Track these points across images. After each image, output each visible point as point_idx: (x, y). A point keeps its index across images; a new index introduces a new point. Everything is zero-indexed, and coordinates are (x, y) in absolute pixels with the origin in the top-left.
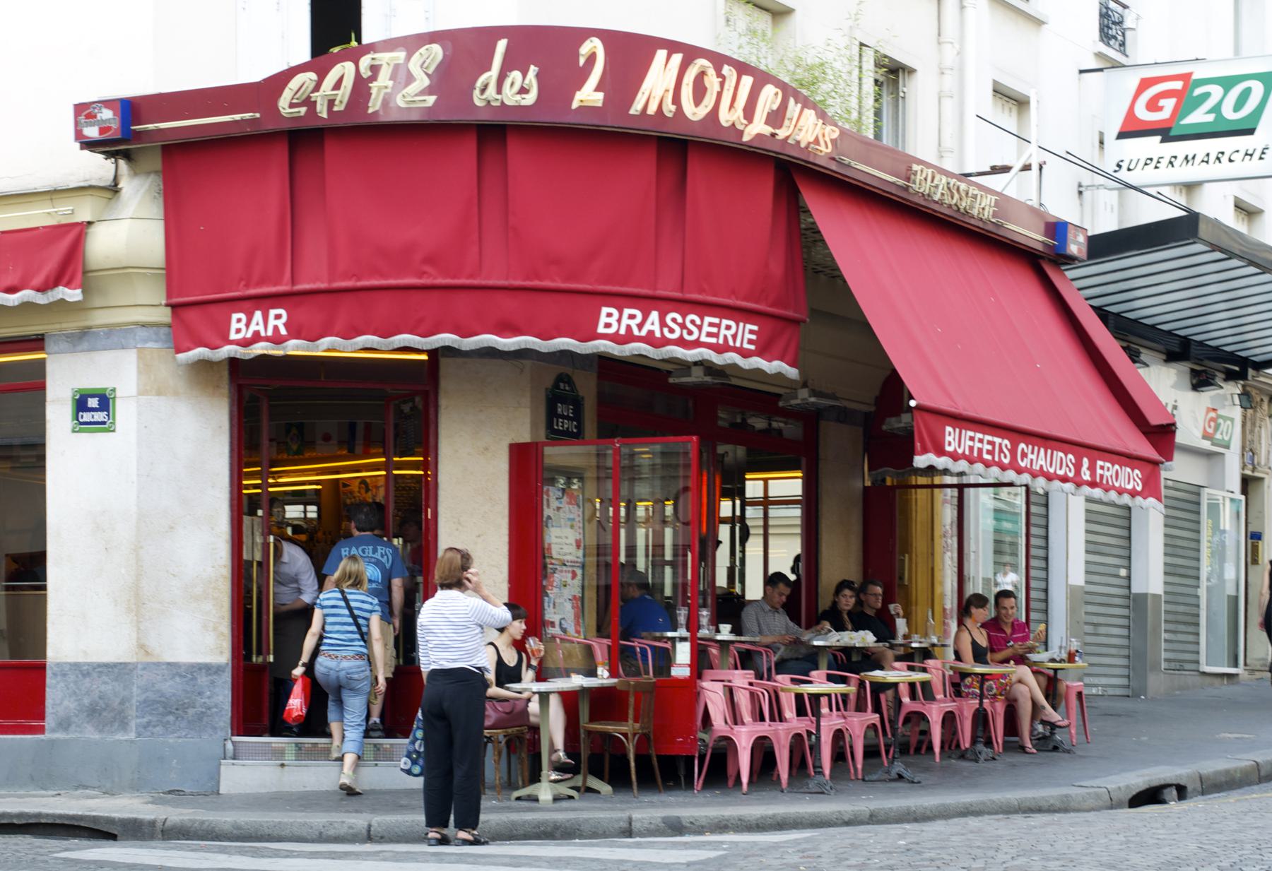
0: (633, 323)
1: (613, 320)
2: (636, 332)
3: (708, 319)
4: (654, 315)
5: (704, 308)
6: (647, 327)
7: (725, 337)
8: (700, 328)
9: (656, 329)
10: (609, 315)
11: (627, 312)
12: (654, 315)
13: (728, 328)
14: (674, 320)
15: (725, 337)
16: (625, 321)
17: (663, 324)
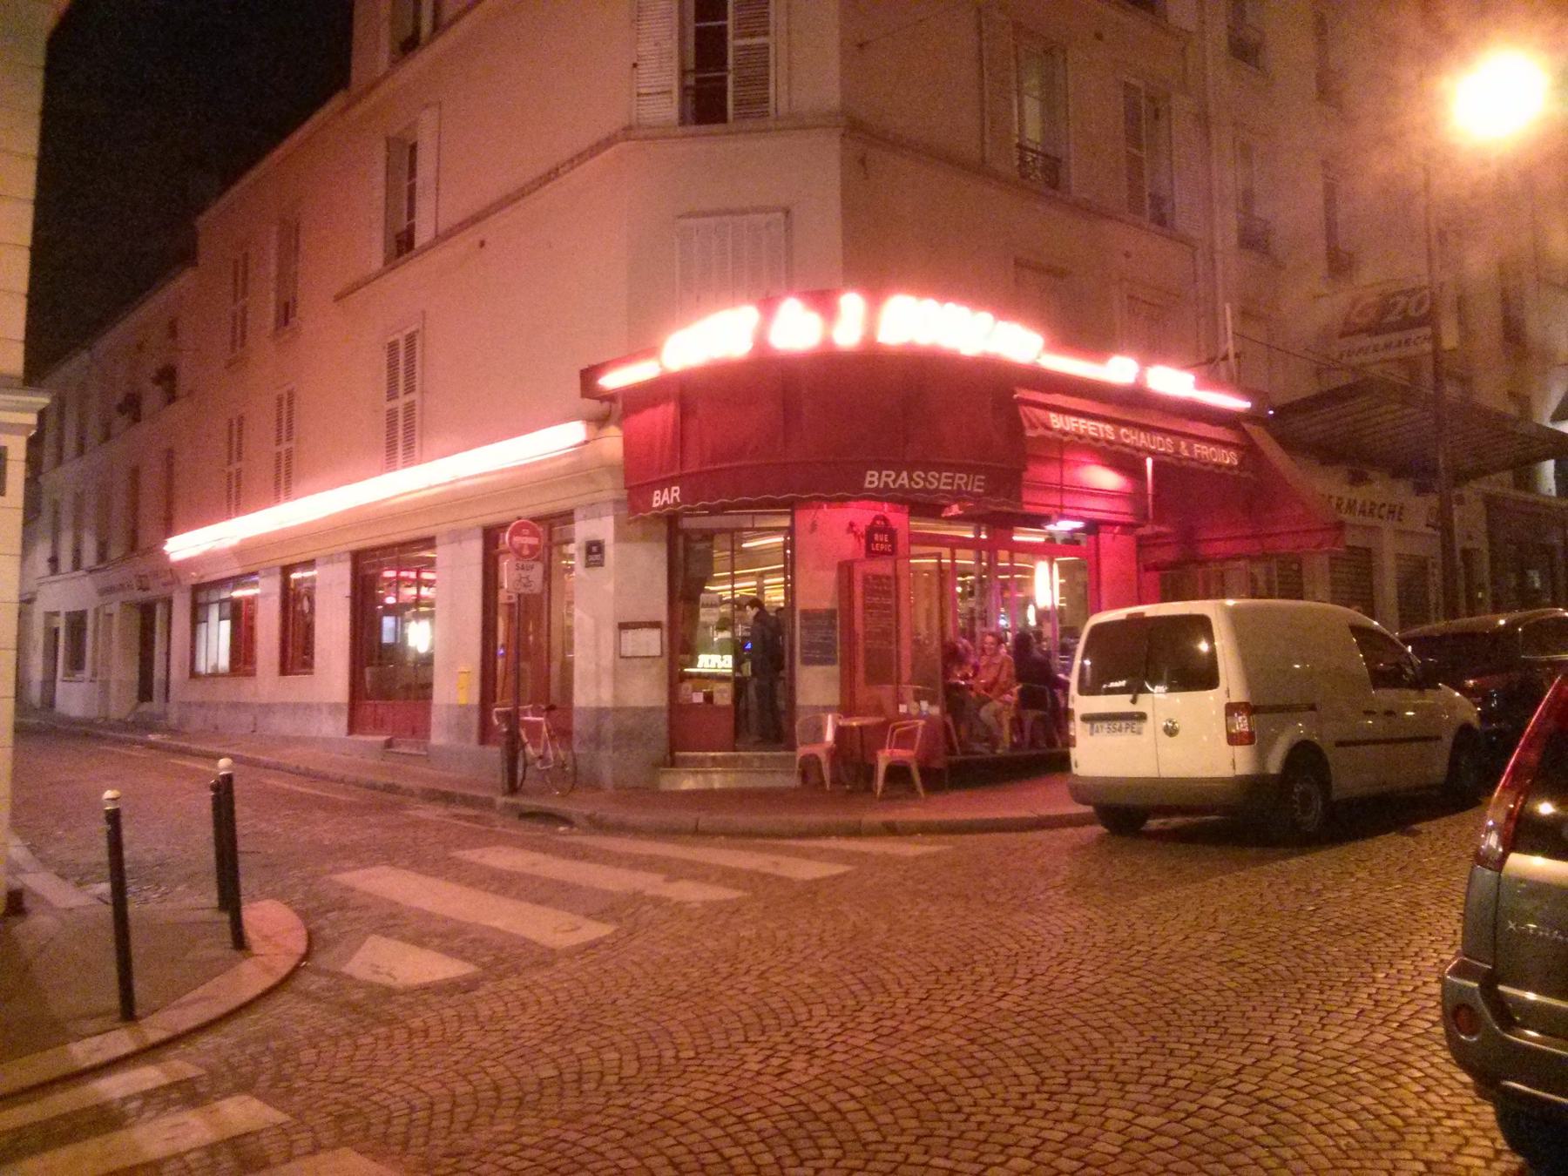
0: (890, 480)
1: (875, 479)
2: (892, 486)
3: (944, 474)
4: (904, 474)
5: (939, 467)
6: (900, 482)
7: (959, 485)
8: (939, 480)
9: (906, 482)
10: (872, 476)
11: (884, 473)
12: (904, 474)
13: (961, 478)
14: (919, 476)
15: (959, 485)
16: (884, 479)
17: (911, 479)
